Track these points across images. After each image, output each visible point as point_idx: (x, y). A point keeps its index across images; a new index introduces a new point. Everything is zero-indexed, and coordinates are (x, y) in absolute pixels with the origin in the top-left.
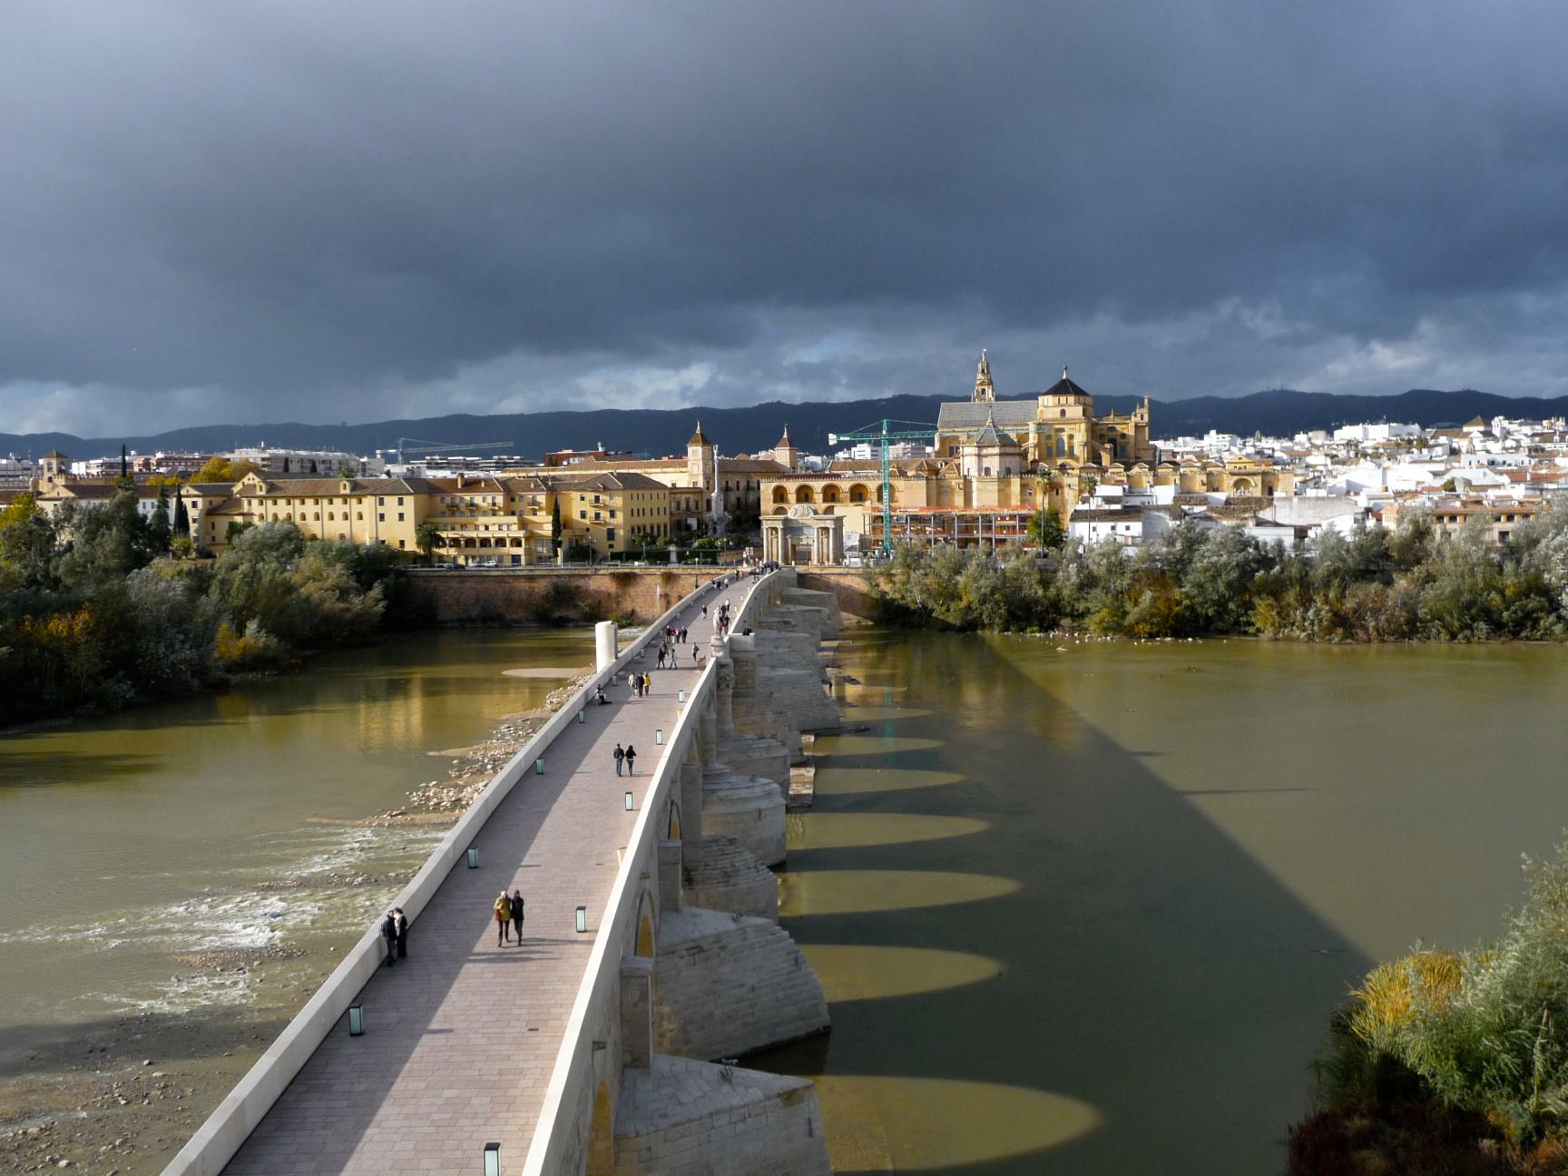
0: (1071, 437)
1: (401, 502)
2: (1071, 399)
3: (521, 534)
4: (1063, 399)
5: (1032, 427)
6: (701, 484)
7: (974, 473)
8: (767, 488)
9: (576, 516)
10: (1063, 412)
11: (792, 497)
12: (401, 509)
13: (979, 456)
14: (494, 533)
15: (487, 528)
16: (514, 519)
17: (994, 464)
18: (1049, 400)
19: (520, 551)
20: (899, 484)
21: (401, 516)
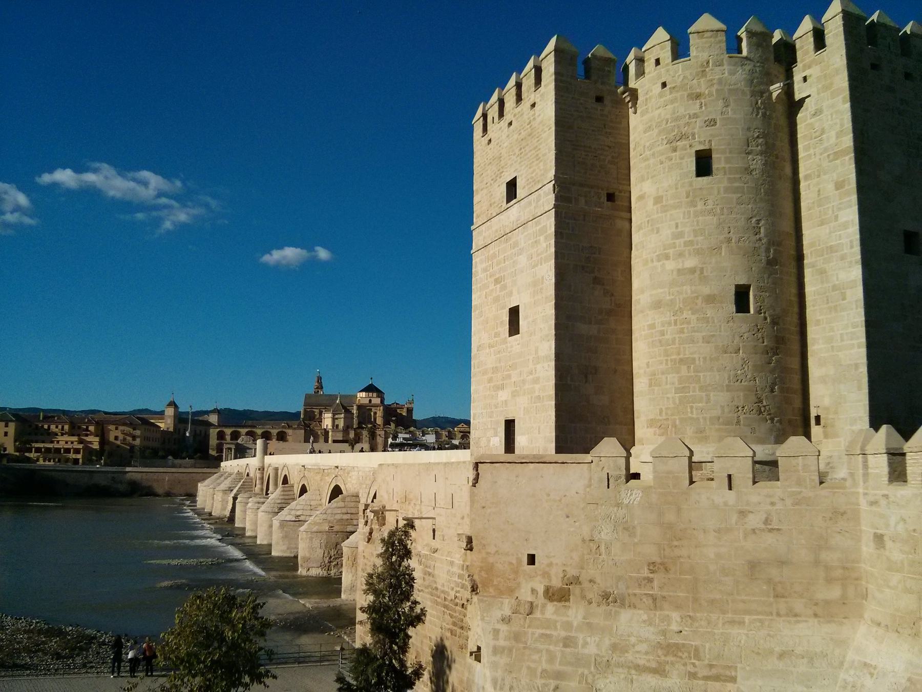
0: (375, 413)
1: (6, 426)
2: (375, 395)
3: (81, 446)
4: (371, 394)
5: (355, 407)
6: (171, 429)
7: (330, 427)
8: (213, 432)
9: (112, 439)
10: (370, 401)
11: (228, 438)
12: (6, 429)
13: (334, 419)
14: (62, 445)
15: (58, 442)
16: (75, 438)
17: (341, 423)
18: (363, 394)
19: (79, 456)
20: (289, 432)
21: (6, 434)
